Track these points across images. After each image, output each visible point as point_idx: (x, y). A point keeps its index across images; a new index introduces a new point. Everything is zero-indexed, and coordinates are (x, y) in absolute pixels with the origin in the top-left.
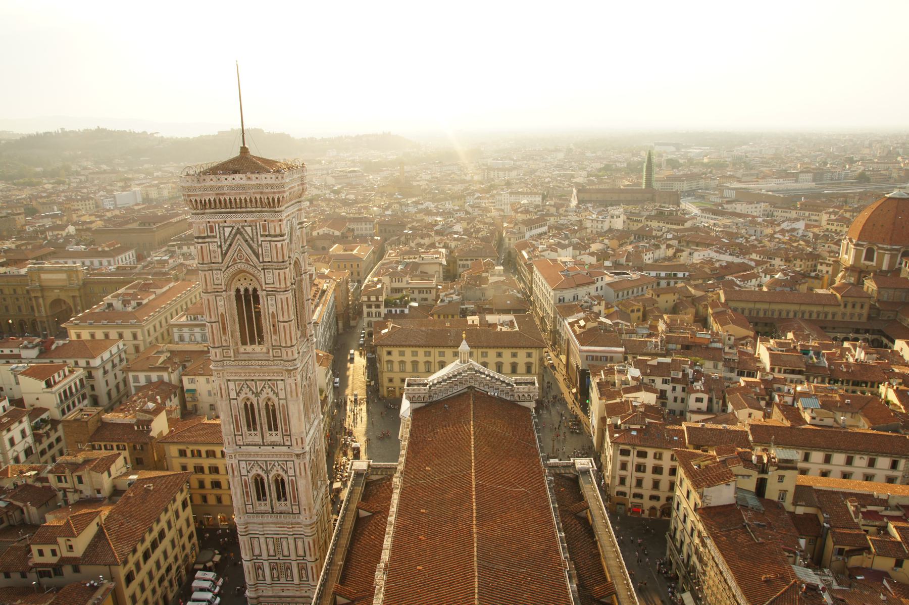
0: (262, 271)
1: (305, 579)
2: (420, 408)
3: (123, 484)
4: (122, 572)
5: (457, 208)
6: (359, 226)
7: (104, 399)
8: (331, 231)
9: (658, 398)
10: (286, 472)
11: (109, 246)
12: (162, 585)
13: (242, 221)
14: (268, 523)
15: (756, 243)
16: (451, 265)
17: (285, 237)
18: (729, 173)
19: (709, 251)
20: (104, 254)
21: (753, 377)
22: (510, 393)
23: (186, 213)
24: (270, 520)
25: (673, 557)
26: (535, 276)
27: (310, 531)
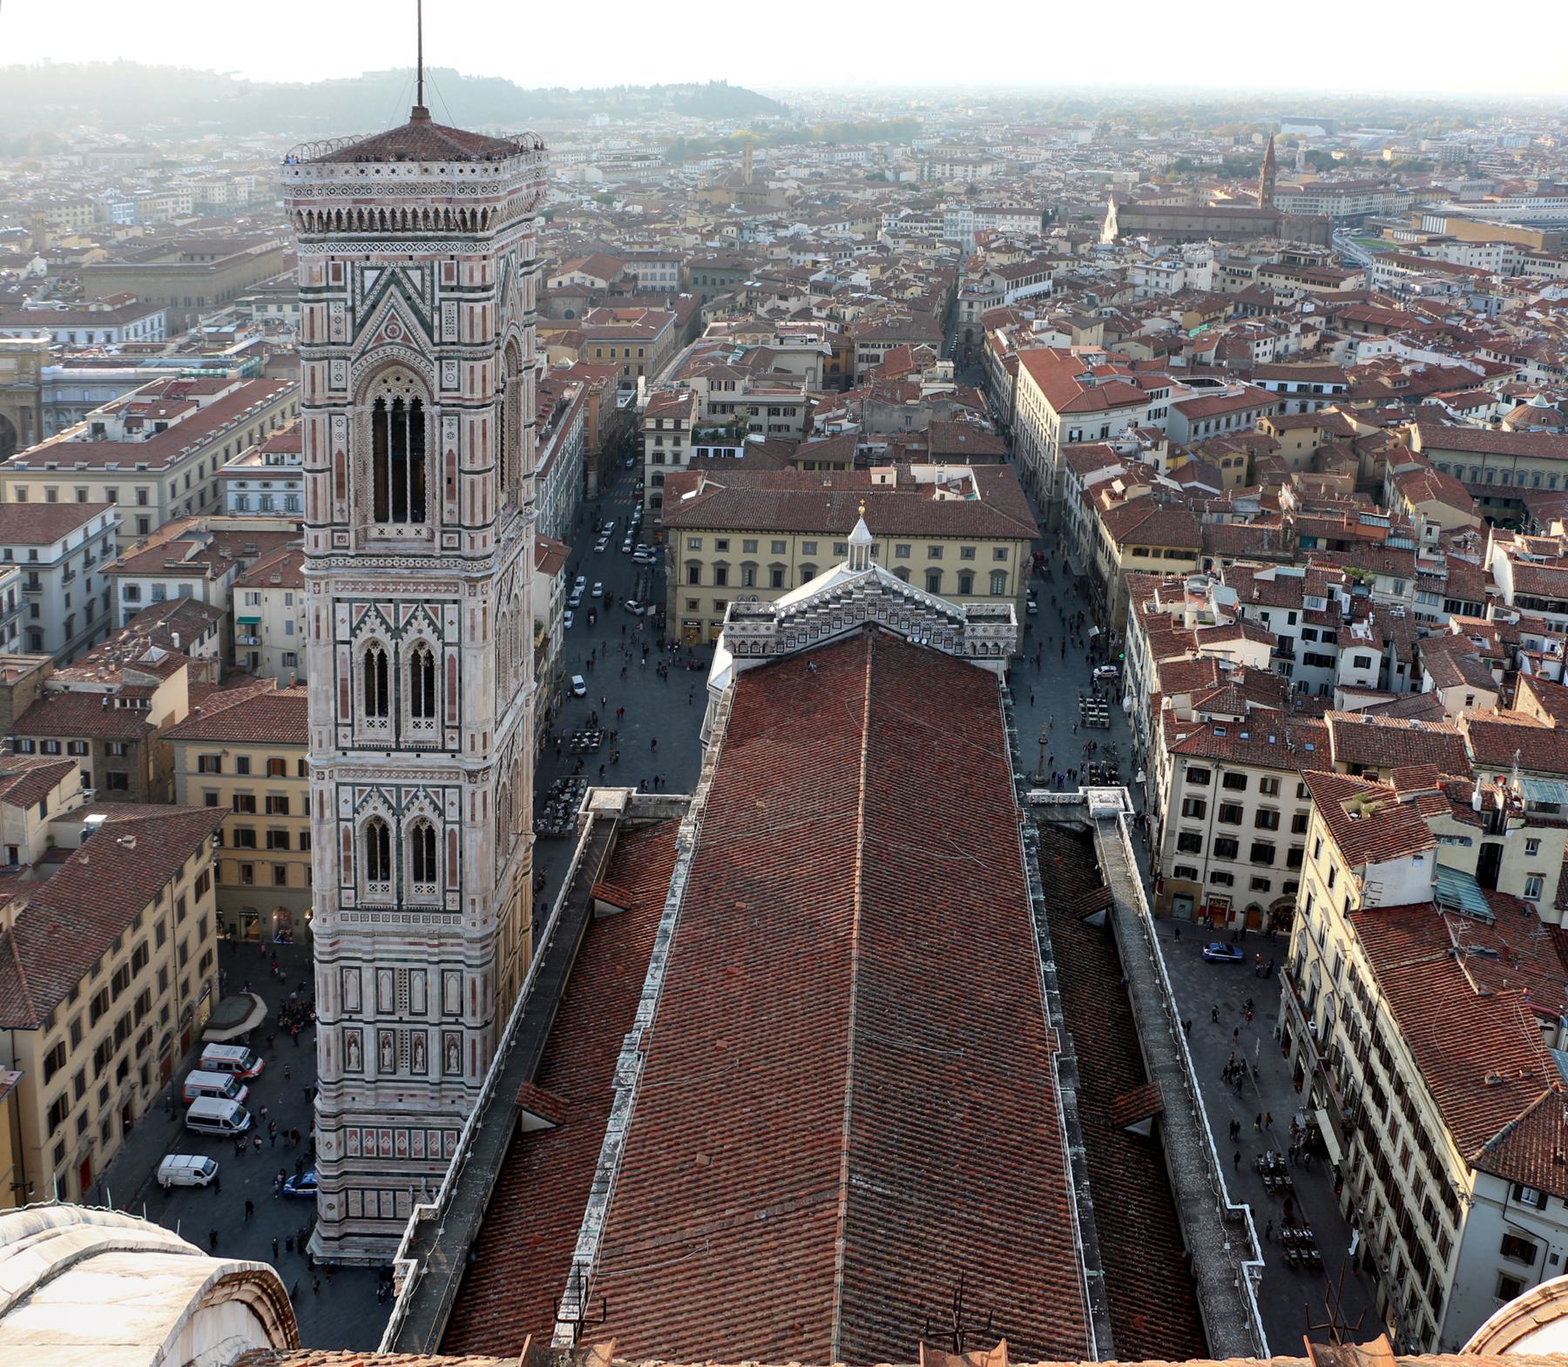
0: (437, 363)
1: (454, 1070)
2: (756, 669)
3: (69, 834)
4: (37, 1045)
5: (860, 237)
6: (649, 271)
7: (55, 637)
8: (587, 280)
9: (1274, 655)
10: (442, 813)
11: (112, 302)
12: (125, 1079)
13: (402, 258)
14: (386, 934)
15: (1487, 326)
16: (843, 355)
17: (491, 293)
18: (1434, 183)
19: (1391, 342)
20: (100, 319)
21: (1477, 615)
22: (955, 640)
23: (281, 234)
24: (391, 926)
25: (1294, 1025)
26: (1020, 385)
27: (478, 953)
